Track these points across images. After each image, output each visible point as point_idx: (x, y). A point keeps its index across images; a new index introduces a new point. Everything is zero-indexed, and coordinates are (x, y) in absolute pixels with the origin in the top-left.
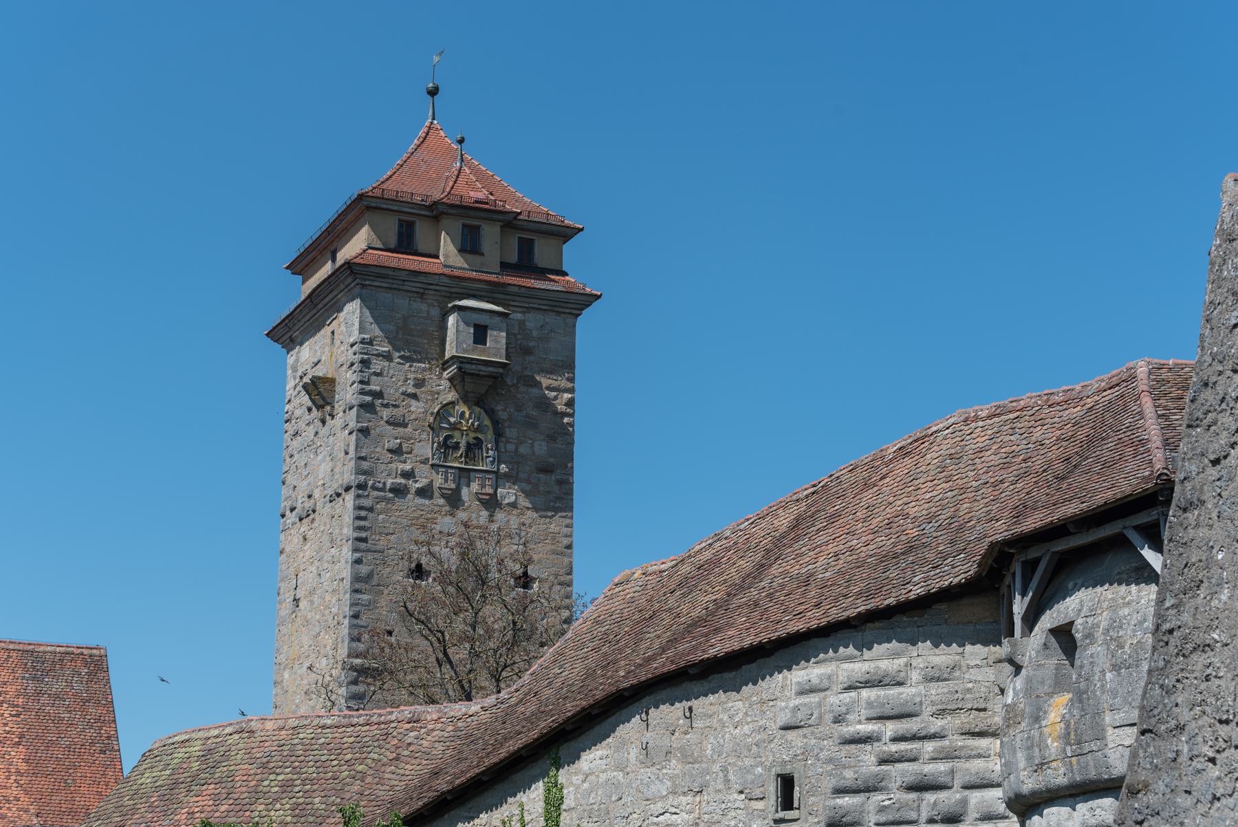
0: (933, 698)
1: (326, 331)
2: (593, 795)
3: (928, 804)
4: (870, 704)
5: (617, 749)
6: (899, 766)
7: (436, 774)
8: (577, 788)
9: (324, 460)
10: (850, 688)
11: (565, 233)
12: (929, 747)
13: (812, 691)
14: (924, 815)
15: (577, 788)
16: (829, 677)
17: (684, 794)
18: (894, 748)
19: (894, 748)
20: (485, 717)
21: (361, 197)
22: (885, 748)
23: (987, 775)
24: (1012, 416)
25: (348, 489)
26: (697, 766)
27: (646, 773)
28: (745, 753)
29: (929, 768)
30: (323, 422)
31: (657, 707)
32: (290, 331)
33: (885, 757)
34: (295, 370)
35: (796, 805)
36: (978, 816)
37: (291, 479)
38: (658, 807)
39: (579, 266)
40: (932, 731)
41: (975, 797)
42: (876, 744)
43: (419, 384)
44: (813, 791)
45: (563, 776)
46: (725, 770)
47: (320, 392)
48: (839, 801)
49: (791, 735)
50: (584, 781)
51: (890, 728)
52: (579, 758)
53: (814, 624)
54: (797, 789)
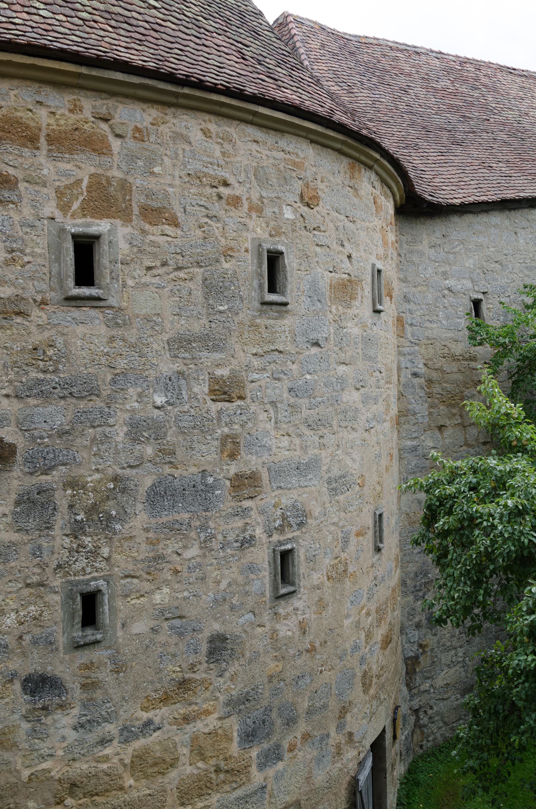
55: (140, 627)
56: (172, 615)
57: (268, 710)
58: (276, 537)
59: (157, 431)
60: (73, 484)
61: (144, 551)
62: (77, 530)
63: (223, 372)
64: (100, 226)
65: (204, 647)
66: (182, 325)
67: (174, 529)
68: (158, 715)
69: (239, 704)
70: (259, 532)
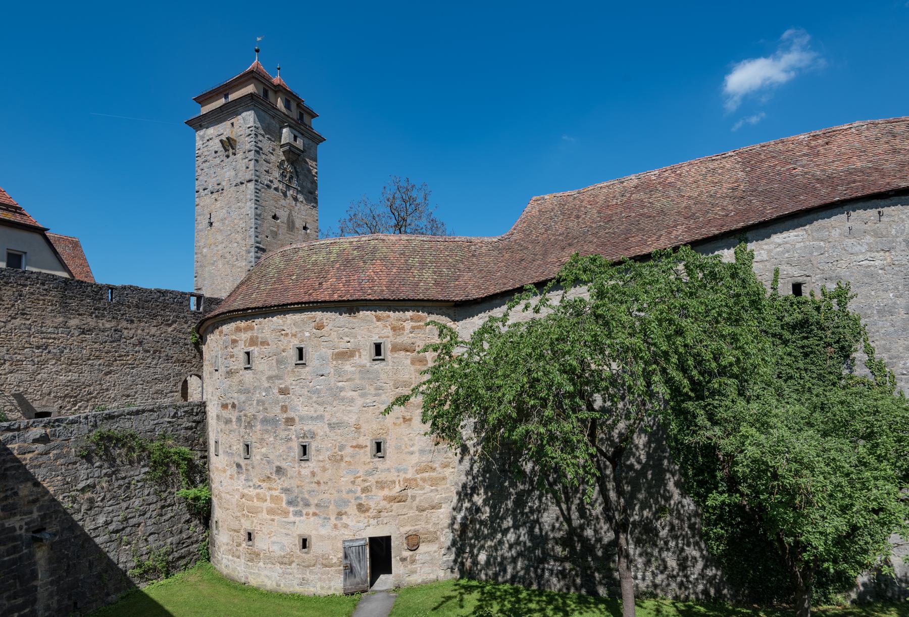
1: (228, 123)
8: (769, 251)
9: (229, 170)
11: (313, 115)
15: (769, 251)
25: (249, 181)
30: (228, 156)
31: (854, 211)
32: (199, 123)
34: (202, 137)
37: (200, 178)
38: (861, 257)
39: (316, 125)
43: (274, 150)
45: (751, 246)
47: (229, 144)
52: (769, 237)
55: (258, 457)
56: (266, 456)
57: (297, 497)
58: (301, 440)
59: (263, 403)
60: (245, 415)
61: (259, 436)
62: (246, 428)
63: (283, 386)
64: (250, 349)
65: (275, 469)
66: (271, 373)
67: (267, 431)
68: (264, 485)
69: (286, 490)
70: (293, 437)
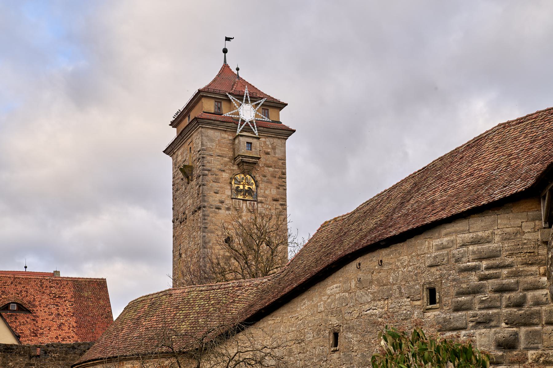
0: (506, 248)
2: (333, 305)
3: (506, 298)
4: (474, 252)
5: (345, 283)
6: (490, 281)
7: (251, 306)
8: (325, 302)
10: (463, 245)
12: (505, 272)
13: (443, 248)
14: (504, 303)
15: (325, 302)
16: (452, 241)
17: (379, 300)
18: (487, 272)
19: (487, 272)
20: (269, 283)
21: (199, 91)
22: (482, 273)
23: (536, 284)
24: (531, 121)
26: (385, 287)
27: (359, 293)
28: (410, 279)
29: (505, 281)
33: (483, 277)
35: (437, 301)
36: (532, 303)
38: (367, 307)
40: (507, 264)
41: (530, 295)
42: (477, 271)
44: (447, 294)
46: (399, 288)
48: (460, 299)
49: (433, 270)
50: (328, 299)
51: (484, 264)
53: (444, 216)
54: (437, 294)
